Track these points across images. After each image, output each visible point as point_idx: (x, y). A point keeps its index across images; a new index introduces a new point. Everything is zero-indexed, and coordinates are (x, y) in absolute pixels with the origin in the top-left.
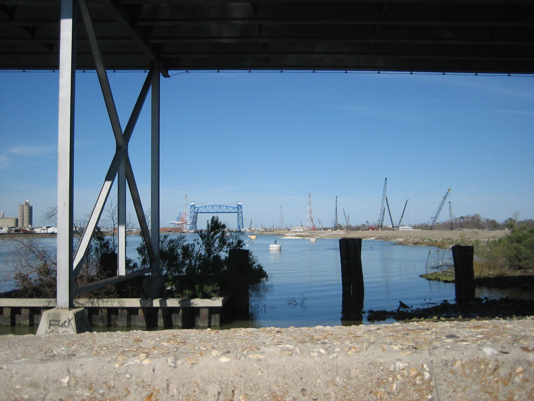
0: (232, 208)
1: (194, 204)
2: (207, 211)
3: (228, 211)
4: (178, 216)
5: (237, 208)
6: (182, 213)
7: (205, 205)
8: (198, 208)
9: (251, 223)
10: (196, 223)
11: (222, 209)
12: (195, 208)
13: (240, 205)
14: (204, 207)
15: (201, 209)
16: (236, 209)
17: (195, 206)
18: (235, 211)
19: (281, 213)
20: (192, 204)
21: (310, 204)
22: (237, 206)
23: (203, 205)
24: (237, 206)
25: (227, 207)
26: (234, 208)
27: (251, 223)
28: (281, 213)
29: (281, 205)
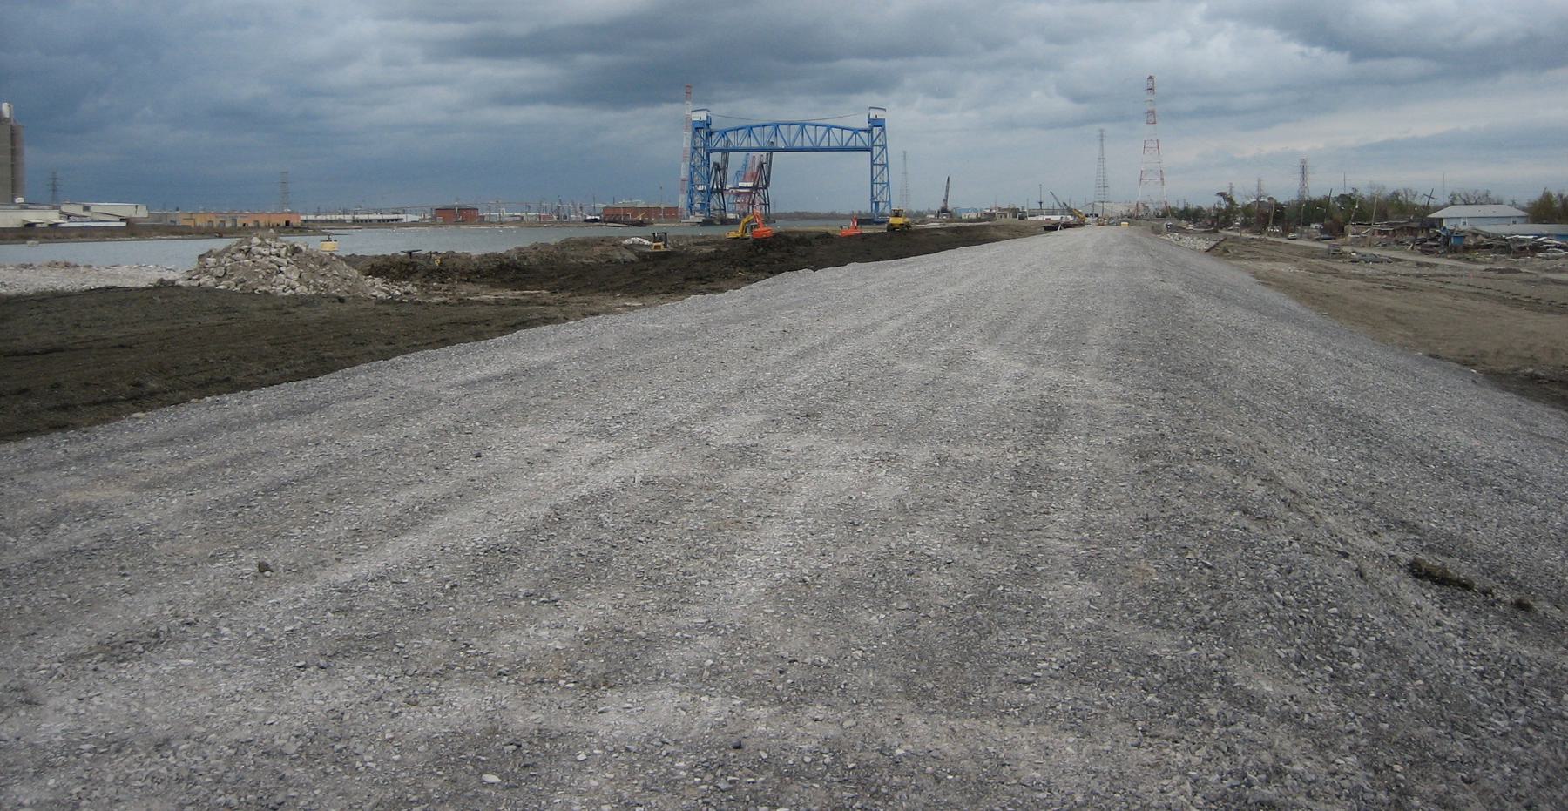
1: (704, 118)
3: (833, 144)
5: (869, 131)
8: (724, 133)
9: (947, 191)
11: (812, 136)
12: (712, 133)
13: (876, 119)
15: (731, 136)
17: (713, 127)
18: (860, 144)
20: (696, 117)
21: (1152, 118)
23: (743, 123)
24: (867, 126)
26: (856, 131)
27: (947, 191)
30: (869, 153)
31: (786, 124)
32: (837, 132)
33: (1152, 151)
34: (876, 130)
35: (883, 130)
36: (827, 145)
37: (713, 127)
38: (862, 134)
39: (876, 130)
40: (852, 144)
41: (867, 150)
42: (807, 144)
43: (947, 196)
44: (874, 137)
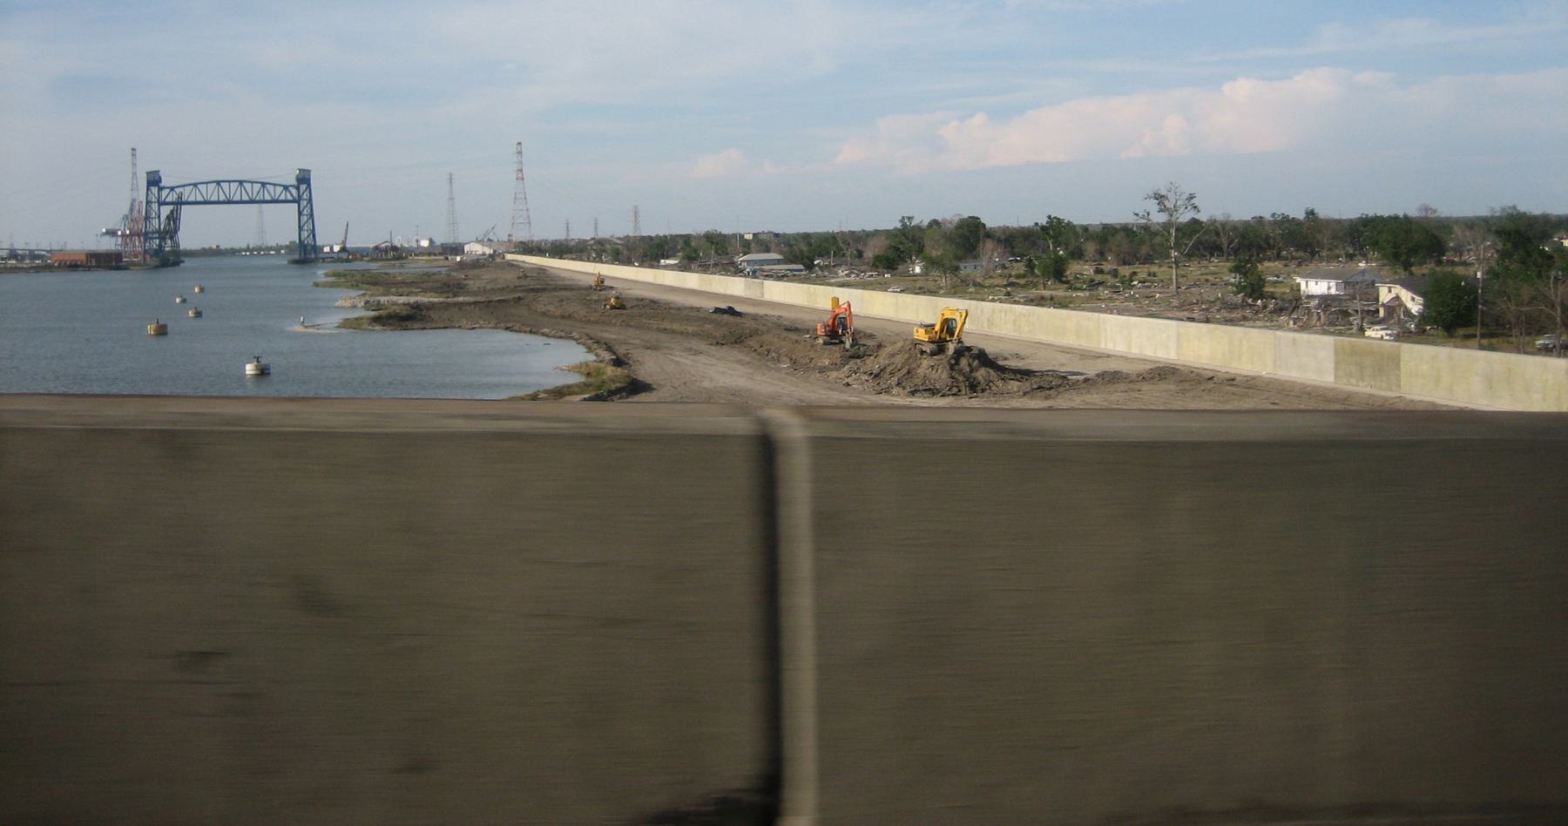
0: (279, 189)
2: (200, 199)
4: (126, 210)
5: (298, 188)
6: (137, 203)
7: (193, 182)
8: (172, 189)
9: (346, 233)
10: (176, 230)
12: (161, 189)
14: (190, 185)
16: (294, 191)
17: (162, 185)
18: (290, 198)
19: (452, 199)
21: (520, 175)
22: (294, 182)
25: (263, 184)
26: (286, 188)
27: (346, 233)
28: (452, 199)
29: (451, 175)
30: (297, 205)
31: (249, 182)
32: (271, 188)
33: (520, 201)
34: (303, 187)
35: (309, 186)
36: (262, 198)
37: (162, 185)
38: (290, 188)
39: (303, 187)
40: (282, 198)
41: (293, 201)
42: (245, 198)
43: (346, 238)
44: (301, 193)
